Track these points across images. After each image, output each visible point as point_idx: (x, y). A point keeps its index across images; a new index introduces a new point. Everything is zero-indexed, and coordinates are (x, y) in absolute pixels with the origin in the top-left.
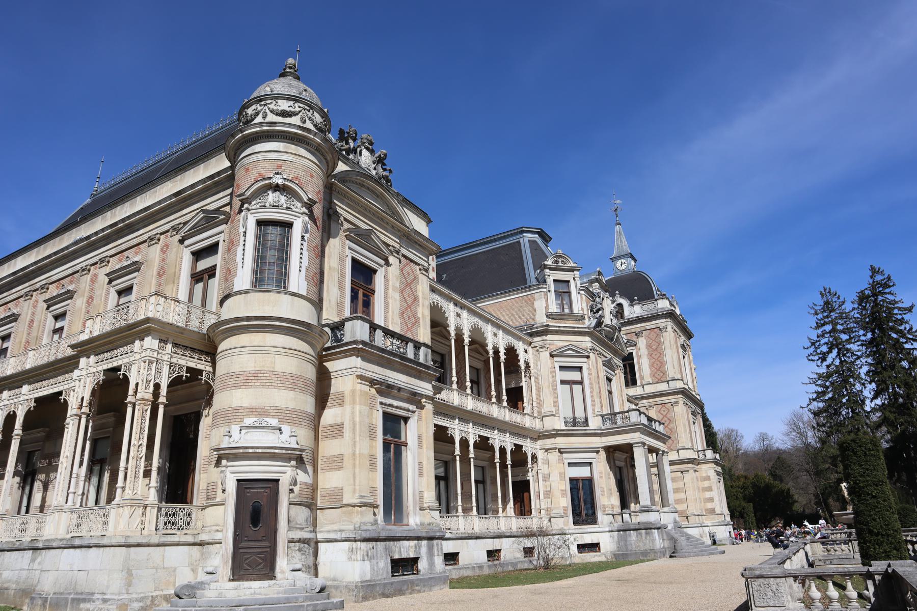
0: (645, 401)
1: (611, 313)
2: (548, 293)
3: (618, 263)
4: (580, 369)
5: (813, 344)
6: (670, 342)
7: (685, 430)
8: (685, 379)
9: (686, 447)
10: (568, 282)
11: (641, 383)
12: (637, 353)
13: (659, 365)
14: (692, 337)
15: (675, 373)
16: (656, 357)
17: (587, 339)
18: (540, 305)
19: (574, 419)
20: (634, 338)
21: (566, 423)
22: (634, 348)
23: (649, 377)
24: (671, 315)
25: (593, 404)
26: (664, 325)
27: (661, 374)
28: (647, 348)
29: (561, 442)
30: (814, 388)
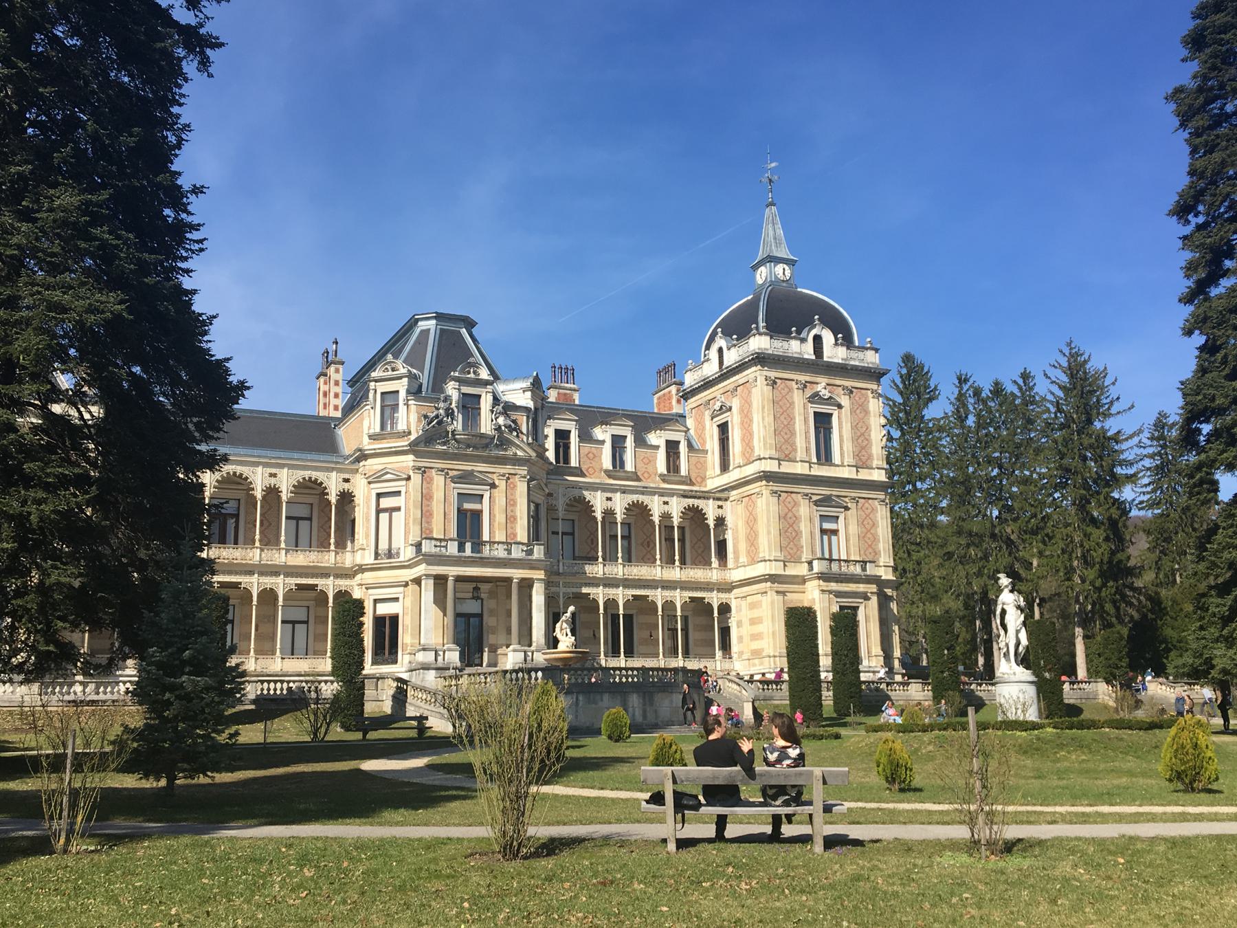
0: (734, 492)
1: (492, 412)
2: (372, 411)
4: (398, 493)
7: (769, 533)
8: (800, 454)
10: (398, 392)
14: (884, 374)
16: (746, 426)
17: (411, 457)
18: (366, 423)
19: (390, 550)
21: (377, 555)
22: (728, 413)
24: (760, 359)
25: (407, 533)
26: (752, 376)
29: (368, 577)
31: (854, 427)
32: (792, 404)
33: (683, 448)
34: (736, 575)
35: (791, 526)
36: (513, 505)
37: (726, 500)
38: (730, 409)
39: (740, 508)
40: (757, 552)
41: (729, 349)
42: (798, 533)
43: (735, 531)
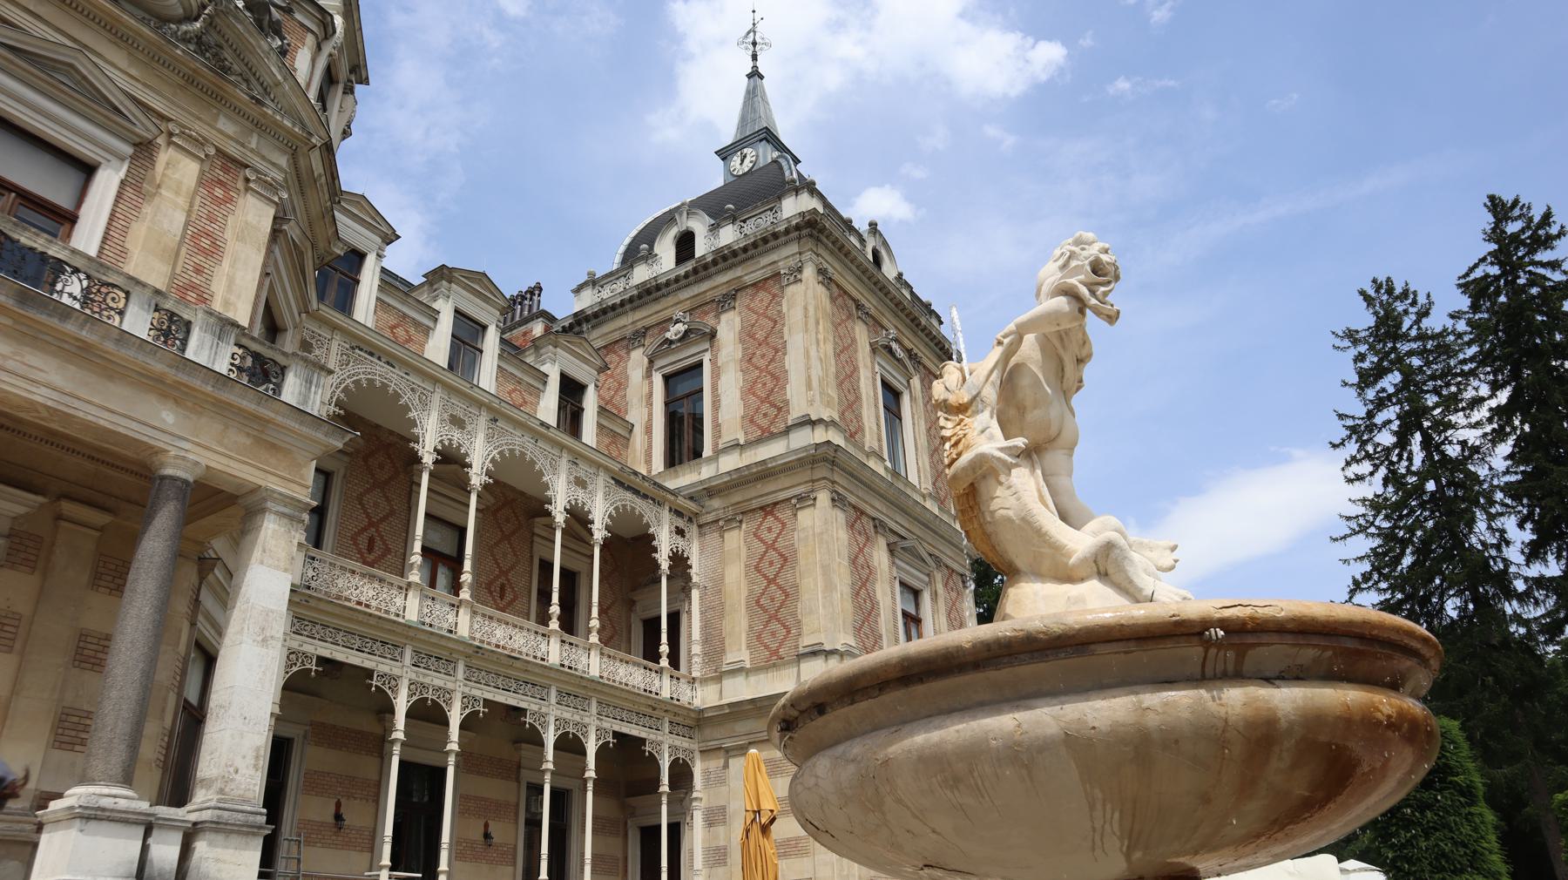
0: (716, 503)
3: (736, 159)
5: (1353, 430)
6: (806, 308)
7: (829, 587)
8: (870, 441)
9: (827, 647)
11: (715, 445)
12: (713, 361)
13: (770, 385)
15: (811, 402)
16: (762, 363)
20: (710, 320)
22: (707, 345)
23: (739, 427)
26: (792, 262)
27: (773, 412)
28: (742, 341)
30: (1364, 544)
31: (929, 430)
32: (854, 340)
33: (590, 402)
34: (705, 697)
35: (864, 585)
36: (207, 253)
37: (690, 520)
38: (713, 335)
39: (735, 539)
40: (791, 628)
41: (714, 229)
42: (874, 605)
43: (716, 588)
